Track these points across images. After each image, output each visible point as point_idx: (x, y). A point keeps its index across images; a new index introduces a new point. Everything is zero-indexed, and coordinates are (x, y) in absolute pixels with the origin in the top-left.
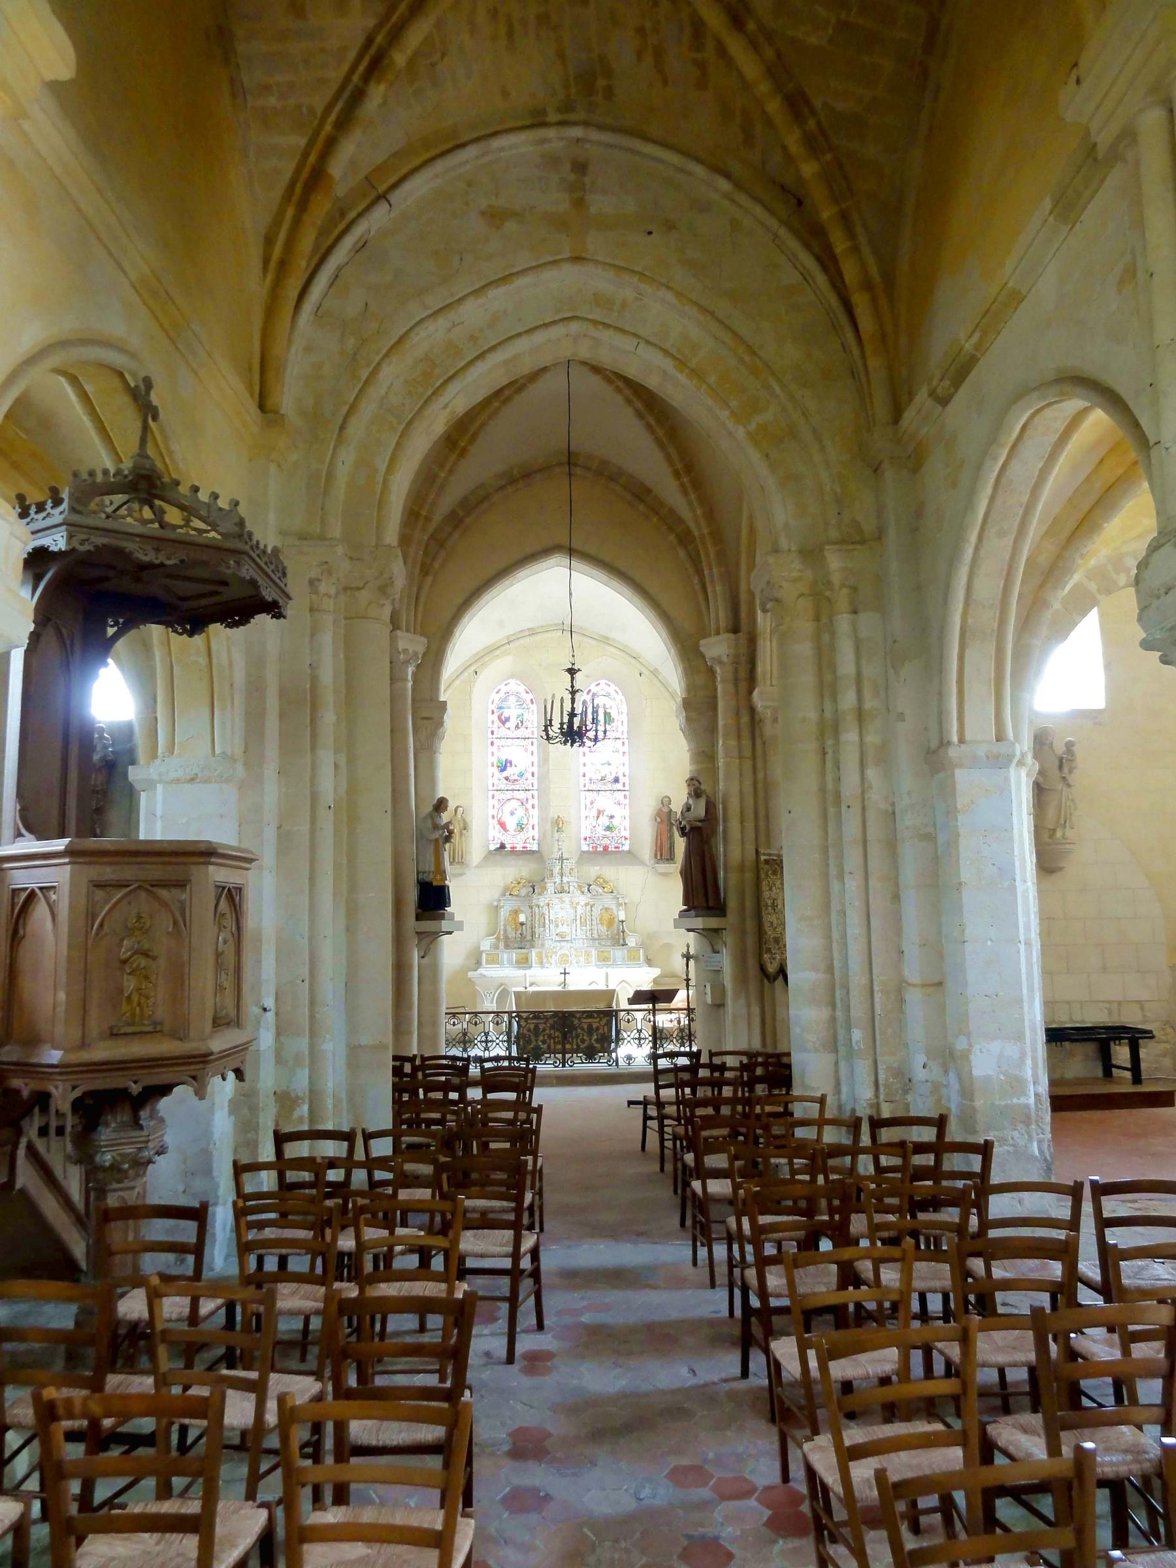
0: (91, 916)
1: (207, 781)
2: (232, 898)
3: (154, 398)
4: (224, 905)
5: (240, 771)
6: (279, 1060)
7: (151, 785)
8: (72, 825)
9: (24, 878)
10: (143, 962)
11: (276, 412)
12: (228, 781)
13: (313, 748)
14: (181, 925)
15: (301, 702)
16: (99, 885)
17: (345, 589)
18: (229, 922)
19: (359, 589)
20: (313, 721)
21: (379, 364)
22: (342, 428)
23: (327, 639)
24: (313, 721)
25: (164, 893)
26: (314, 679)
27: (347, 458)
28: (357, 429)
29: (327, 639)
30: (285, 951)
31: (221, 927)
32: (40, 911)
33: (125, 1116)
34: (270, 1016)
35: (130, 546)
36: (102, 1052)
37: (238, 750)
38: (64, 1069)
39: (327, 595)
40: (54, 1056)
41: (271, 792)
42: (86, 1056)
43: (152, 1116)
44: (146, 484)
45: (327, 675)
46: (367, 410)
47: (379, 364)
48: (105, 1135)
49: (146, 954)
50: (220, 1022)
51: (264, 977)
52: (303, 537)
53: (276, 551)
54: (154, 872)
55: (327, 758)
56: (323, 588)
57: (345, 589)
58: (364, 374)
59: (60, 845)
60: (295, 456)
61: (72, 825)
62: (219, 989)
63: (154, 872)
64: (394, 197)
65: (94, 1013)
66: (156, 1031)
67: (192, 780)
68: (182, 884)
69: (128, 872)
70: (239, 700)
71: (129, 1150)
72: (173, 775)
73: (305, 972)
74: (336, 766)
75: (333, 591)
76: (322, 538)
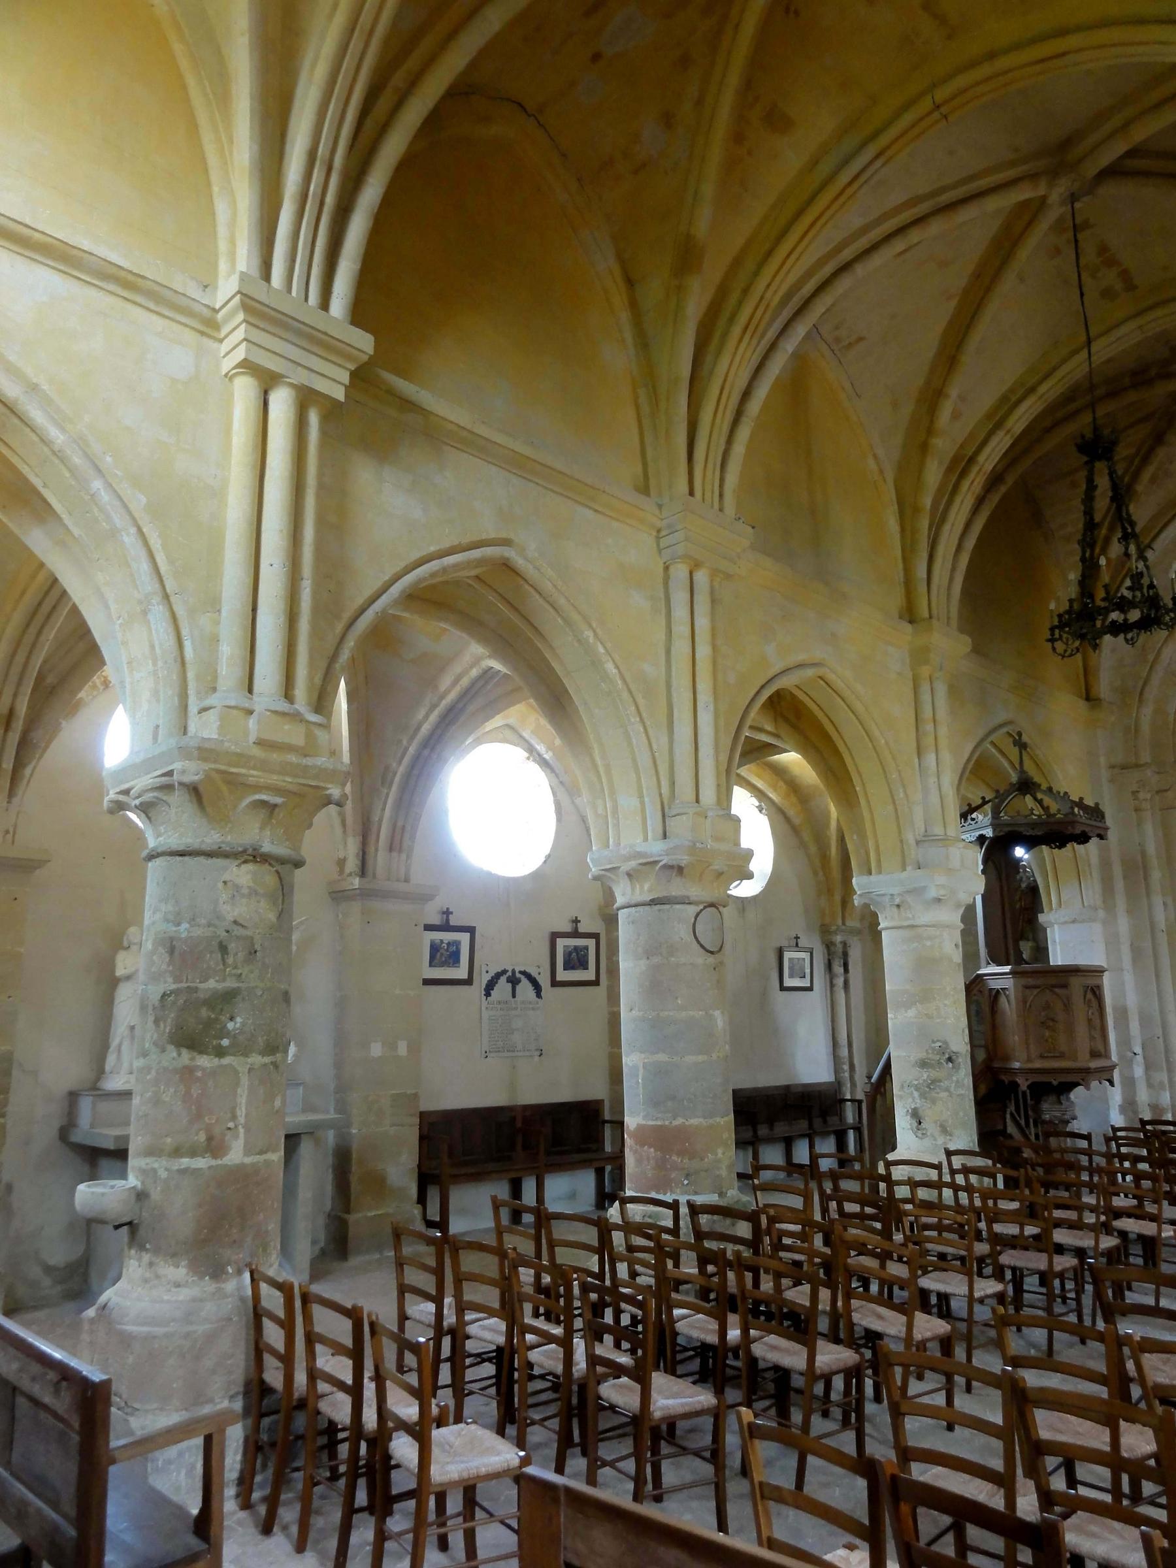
0: (1025, 1002)
1: (1083, 921)
2: (1096, 992)
3: (1025, 738)
4: (1090, 995)
5: (1101, 913)
6: (1150, 1085)
7: (1052, 925)
8: (1012, 958)
9: (995, 984)
10: (1051, 1024)
11: (1099, 700)
12: (1094, 920)
13: (1148, 895)
14: (1067, 1006)
15: (1136, 870)
16: (1027, 987)
17: (1157, 792)
18: (1095, 1003)
19: (1166, 791)
20: (1146, 879)
21: (1161, 648)
22: (1141, 694)
23: (1149, 828)
24: (1146, 879)
25: (1057, 990)
26: (1143, 853)
27: (1147, 711)
28: (1152, 692)
29: (1149, 828)
30: (1145, 1021)
31: (1089, 1007)
32: (1003, 1000)
33: (1052, 1098)
34: (1140, 1058)
35: (1021, 829)
36: (1038, 1064)
37: (1099, 903)
38: (1022, 1071)
39: (1145, 800)
40: (1017, 1065)
41: (1123, 924)
42: (1030, 1066)
43: (1068, 1099)
44: (1026, 786)
45: (1151, 849)
46: (1156, 680)
47: (1161, 648)
48: (1045, 1106)
49: (1053, 1020)
50: (1095, 1054)
51: (1132, 1034)
52: (1124, 767)
53: (1097, 804)
54: (1052, 980)
55: (1158, 900)
56: (1141, 795)
57: (1157, 792)
58: (1151, 657)
59: (1007, 969)
60: (1113, 718)
61: (1012, 958)
62: (1092, 1038)
63: (1052, 980)
64: (1155, 546)
65: (1032, 1046)
66: (1062, 1056)
67: (1074, 922)
68: (1065, 986)
69: (1039, 981)
70: (1096, 874)
71: (1058, 1114)
72: (1062, 920)
73: (1159, 1032)
74: (1165, 904)
75: (1149, 796)
76: (1137, 766)
